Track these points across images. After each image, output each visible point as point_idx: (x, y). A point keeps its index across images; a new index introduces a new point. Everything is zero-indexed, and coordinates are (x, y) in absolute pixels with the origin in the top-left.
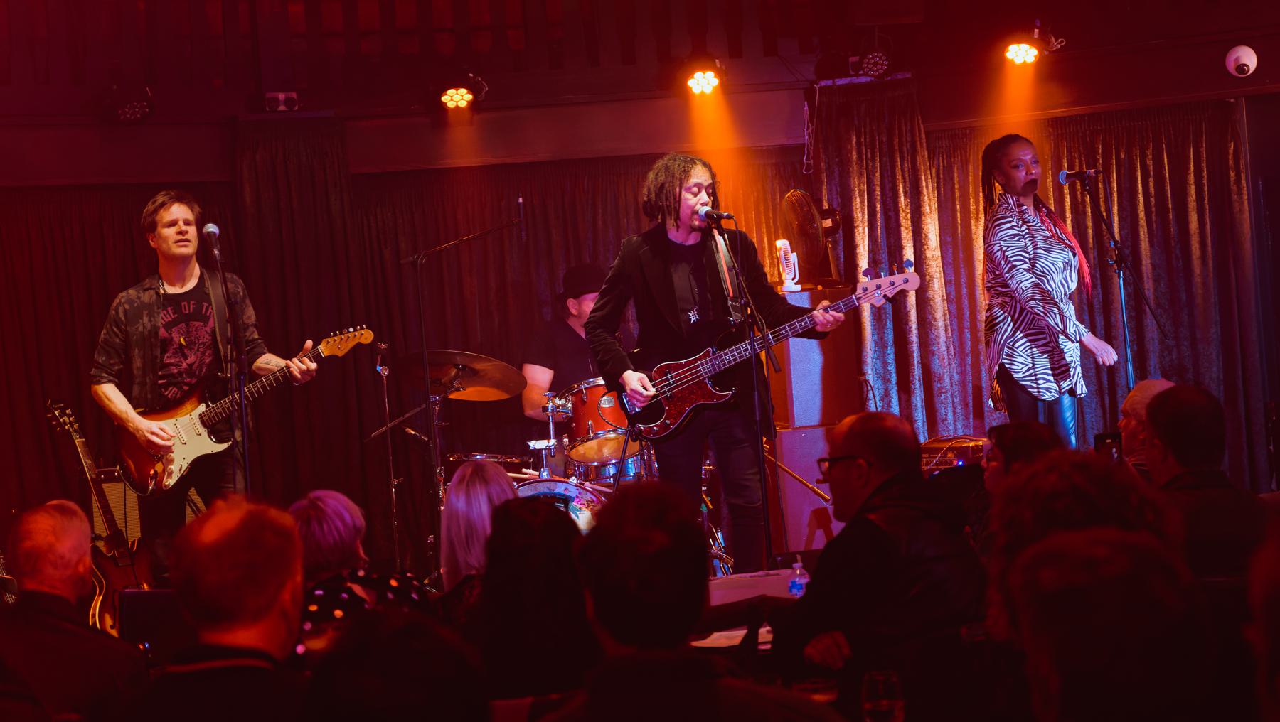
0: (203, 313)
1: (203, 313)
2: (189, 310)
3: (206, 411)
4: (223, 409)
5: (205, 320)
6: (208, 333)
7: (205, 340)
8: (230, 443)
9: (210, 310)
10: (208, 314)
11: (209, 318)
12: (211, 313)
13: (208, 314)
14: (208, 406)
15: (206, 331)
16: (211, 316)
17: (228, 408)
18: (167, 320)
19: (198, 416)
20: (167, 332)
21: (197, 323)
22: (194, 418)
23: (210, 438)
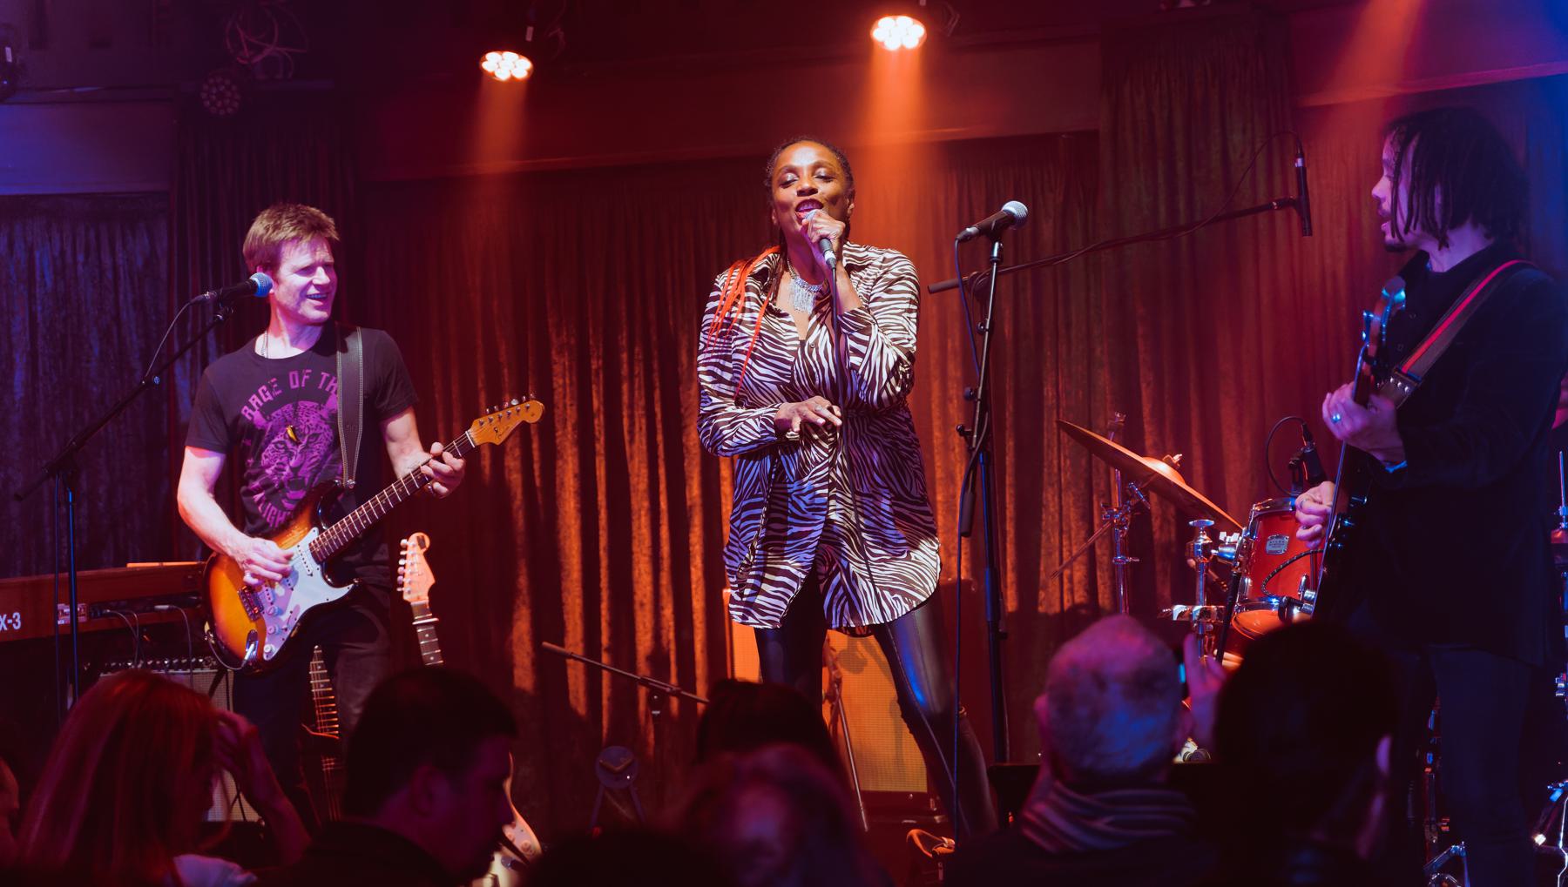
0: (320, 387)
1: (320, 387)
2: (300, 384)
3: (318, 539)
4: (340, 535)
5: (322, 397)
6: (324, 419)
7: (318, 431)
8: (351, 586)
9: (331, 384)
10: (327, 389)
11: (329, 394)
12: (332, 387)
13: (327, 389)
14: (321, 531)
15: (321, 416)
16: (332, 392)
17: (347, 533)
18: (265, 400)
19: (308, 547)
20: (265, 418)
21: (309, 404)
22: (302, 550)
23: (326, 580)
